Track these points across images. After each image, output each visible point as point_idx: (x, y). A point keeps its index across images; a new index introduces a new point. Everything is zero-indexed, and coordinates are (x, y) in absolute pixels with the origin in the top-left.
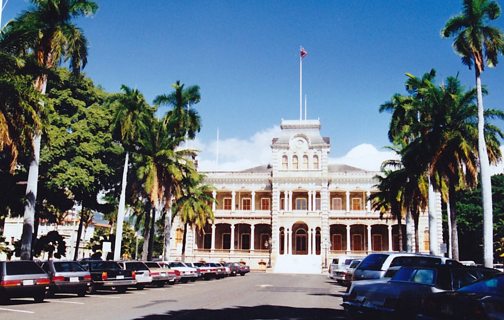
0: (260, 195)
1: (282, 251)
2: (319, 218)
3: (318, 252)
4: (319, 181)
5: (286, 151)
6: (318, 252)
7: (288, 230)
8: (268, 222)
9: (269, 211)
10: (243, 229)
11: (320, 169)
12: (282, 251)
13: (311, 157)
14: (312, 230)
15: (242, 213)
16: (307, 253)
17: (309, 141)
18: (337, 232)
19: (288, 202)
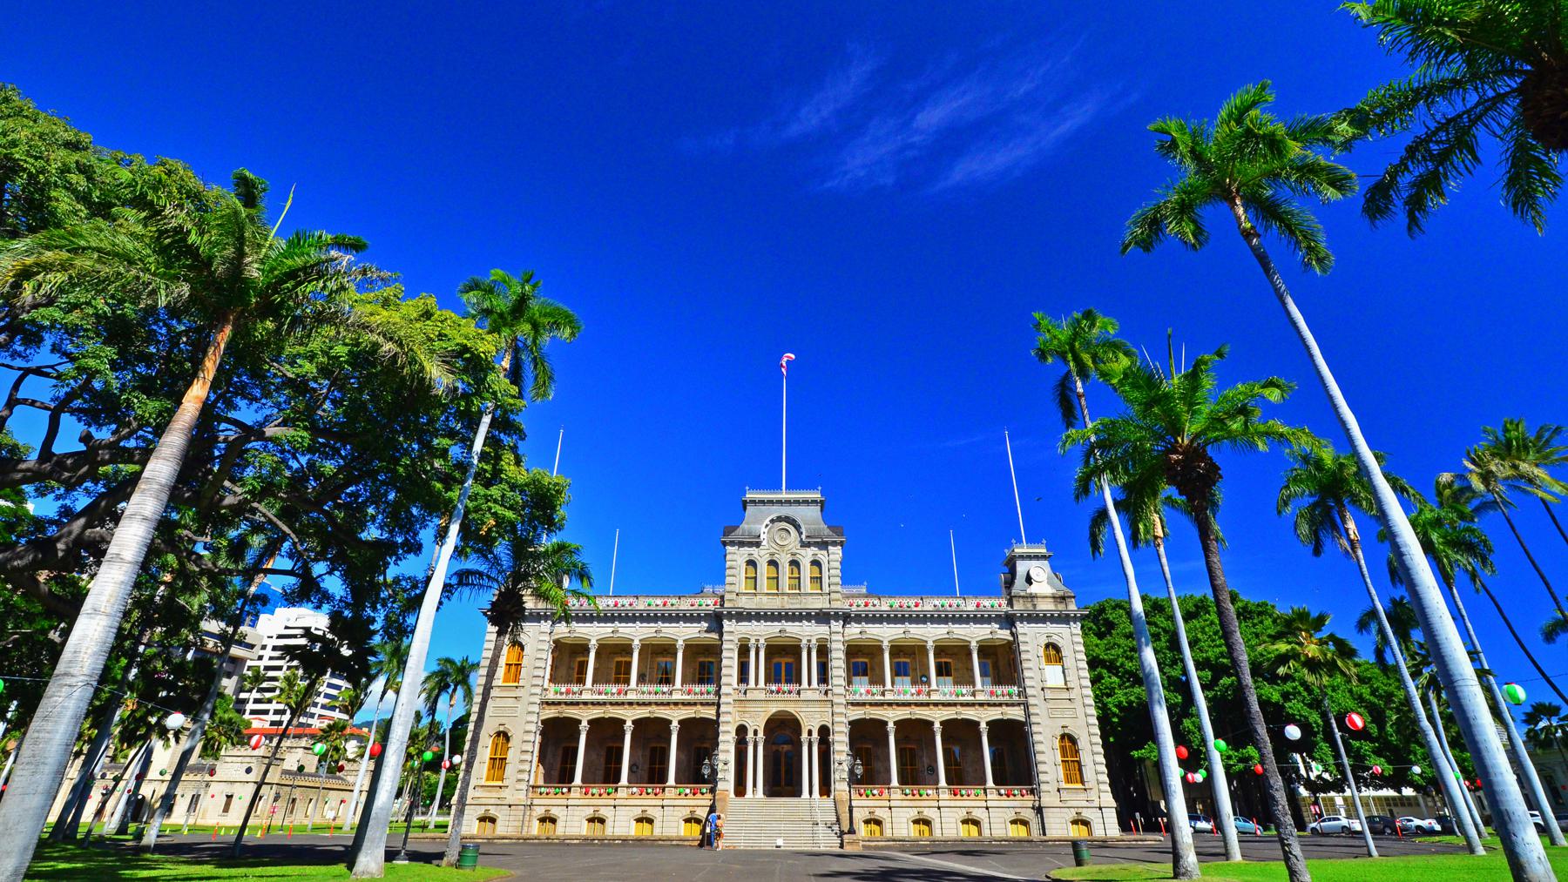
0: (693, 649)
1: (740, 790)
2: (827, 708)
3: (826, 789)
4: (823, 617)
5: (754, 550)
6: (826, 789)
7: (756, 732)
8: (709, 713)
9: (712, 688)
10: (652, 732)
11: (826, 589)
12: (740, 790)
13: (805, 564)
14: (810, 733)
15: (651, 691)
16: (797, 793)
17: (803, 530)
18: (866, 736)
19: (758, 666)
